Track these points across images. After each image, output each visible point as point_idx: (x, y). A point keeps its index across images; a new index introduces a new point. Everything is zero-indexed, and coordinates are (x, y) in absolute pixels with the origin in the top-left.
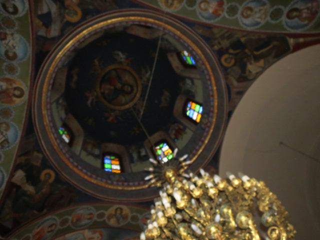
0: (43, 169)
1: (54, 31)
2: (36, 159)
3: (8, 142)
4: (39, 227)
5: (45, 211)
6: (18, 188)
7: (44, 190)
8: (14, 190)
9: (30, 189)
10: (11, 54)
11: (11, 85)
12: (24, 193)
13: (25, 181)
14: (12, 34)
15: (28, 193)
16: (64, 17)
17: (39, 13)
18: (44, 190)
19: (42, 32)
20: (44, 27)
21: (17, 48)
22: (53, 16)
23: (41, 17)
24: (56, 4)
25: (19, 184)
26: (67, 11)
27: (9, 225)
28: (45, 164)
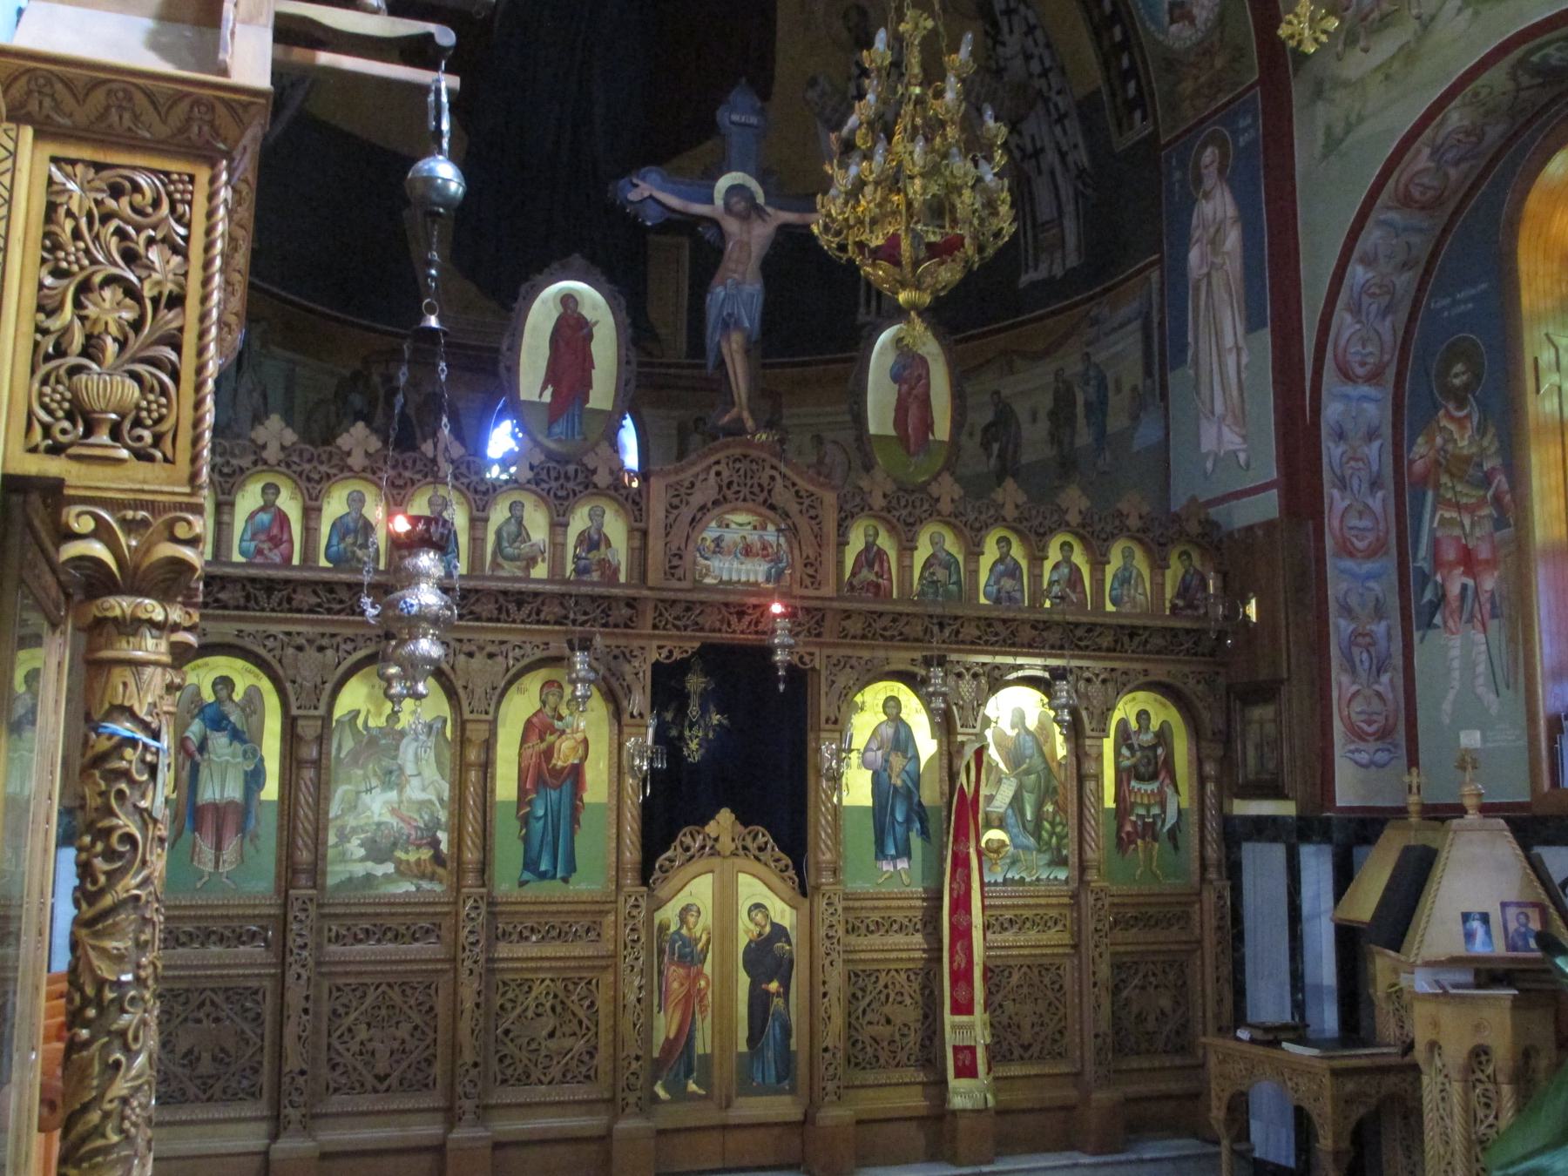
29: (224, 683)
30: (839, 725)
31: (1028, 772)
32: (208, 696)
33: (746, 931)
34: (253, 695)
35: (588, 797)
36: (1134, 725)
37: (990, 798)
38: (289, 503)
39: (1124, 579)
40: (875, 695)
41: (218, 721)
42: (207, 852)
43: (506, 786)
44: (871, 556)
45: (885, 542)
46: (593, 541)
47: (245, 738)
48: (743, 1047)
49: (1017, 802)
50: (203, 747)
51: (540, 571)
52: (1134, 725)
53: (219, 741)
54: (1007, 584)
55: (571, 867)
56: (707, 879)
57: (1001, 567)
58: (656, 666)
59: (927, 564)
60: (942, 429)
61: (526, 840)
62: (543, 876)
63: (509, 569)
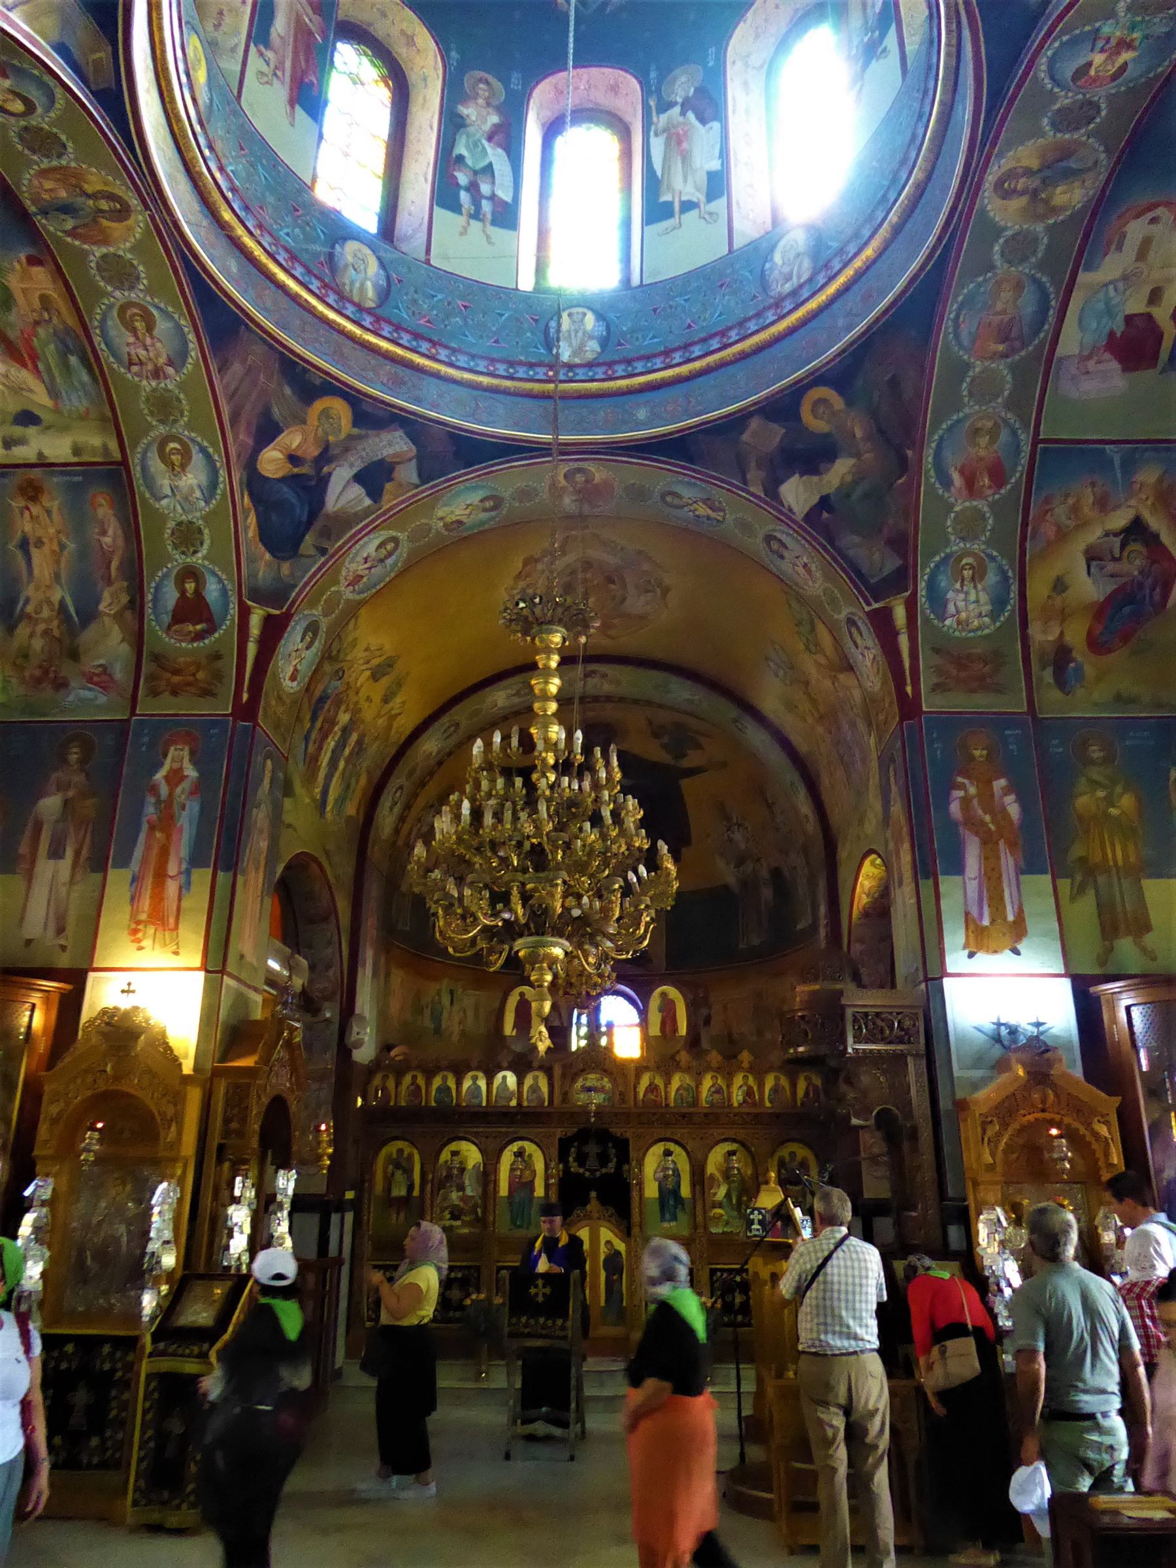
0: (798, 418)
1: (393, 444)
2: (766, 437)
3: (709, 499)
4: (947, 483)
5: (909, 453)
6: (824, 503)
7: (859, 434)
8: (825, 515)
9: (840, 471)
10: (488, 504)
11: (563, 488)
12: (845, 491)
13: (815, 479)
14: (441, 519)
15: (849, 478)
16: (350, 437)
17: (368, 502)
18: (859, 434)
19: (408, 473)
20: (396, 474)
21: (468, 502)
22: (358, 466)
23: (375, 493)
24: (330, 474)
25: (815, 499)
26: (331, 438)
27: (892, 563)
28: (782, 408)
29: (400, 1151)
30: (640, 1164)
31: (733, 1182)
32: (395, 1156)
33: (603, 1251)
34: (410, 1157)
35: (536, 1194)
36: (787, 1158)
37: (715, 1194)
38: (421, 1081)
39: (775, 1090)
40: (658, 1149)
41: (398, 1166)
42: (394, 1216)
43: (504, 1190)
44: (652, 1088)
45: (659, 1082)
46: (535, 1089)
47: (409, 1172)
48: (603, 1303)
49: (728, 1195)
50: (393, 1174)
51: (514, 1103)
52: (787, 1158)
53: (399, 1174)
54: (717, 1096)
55: (529, 1224)
56: (587, 1229)
57: (713, 1089)
58: (560, 1140)
59: (678, 1090)
60: (683, 1030)
61: (512, 1211)
62: (519, 1227)
63: (502, 1103)
